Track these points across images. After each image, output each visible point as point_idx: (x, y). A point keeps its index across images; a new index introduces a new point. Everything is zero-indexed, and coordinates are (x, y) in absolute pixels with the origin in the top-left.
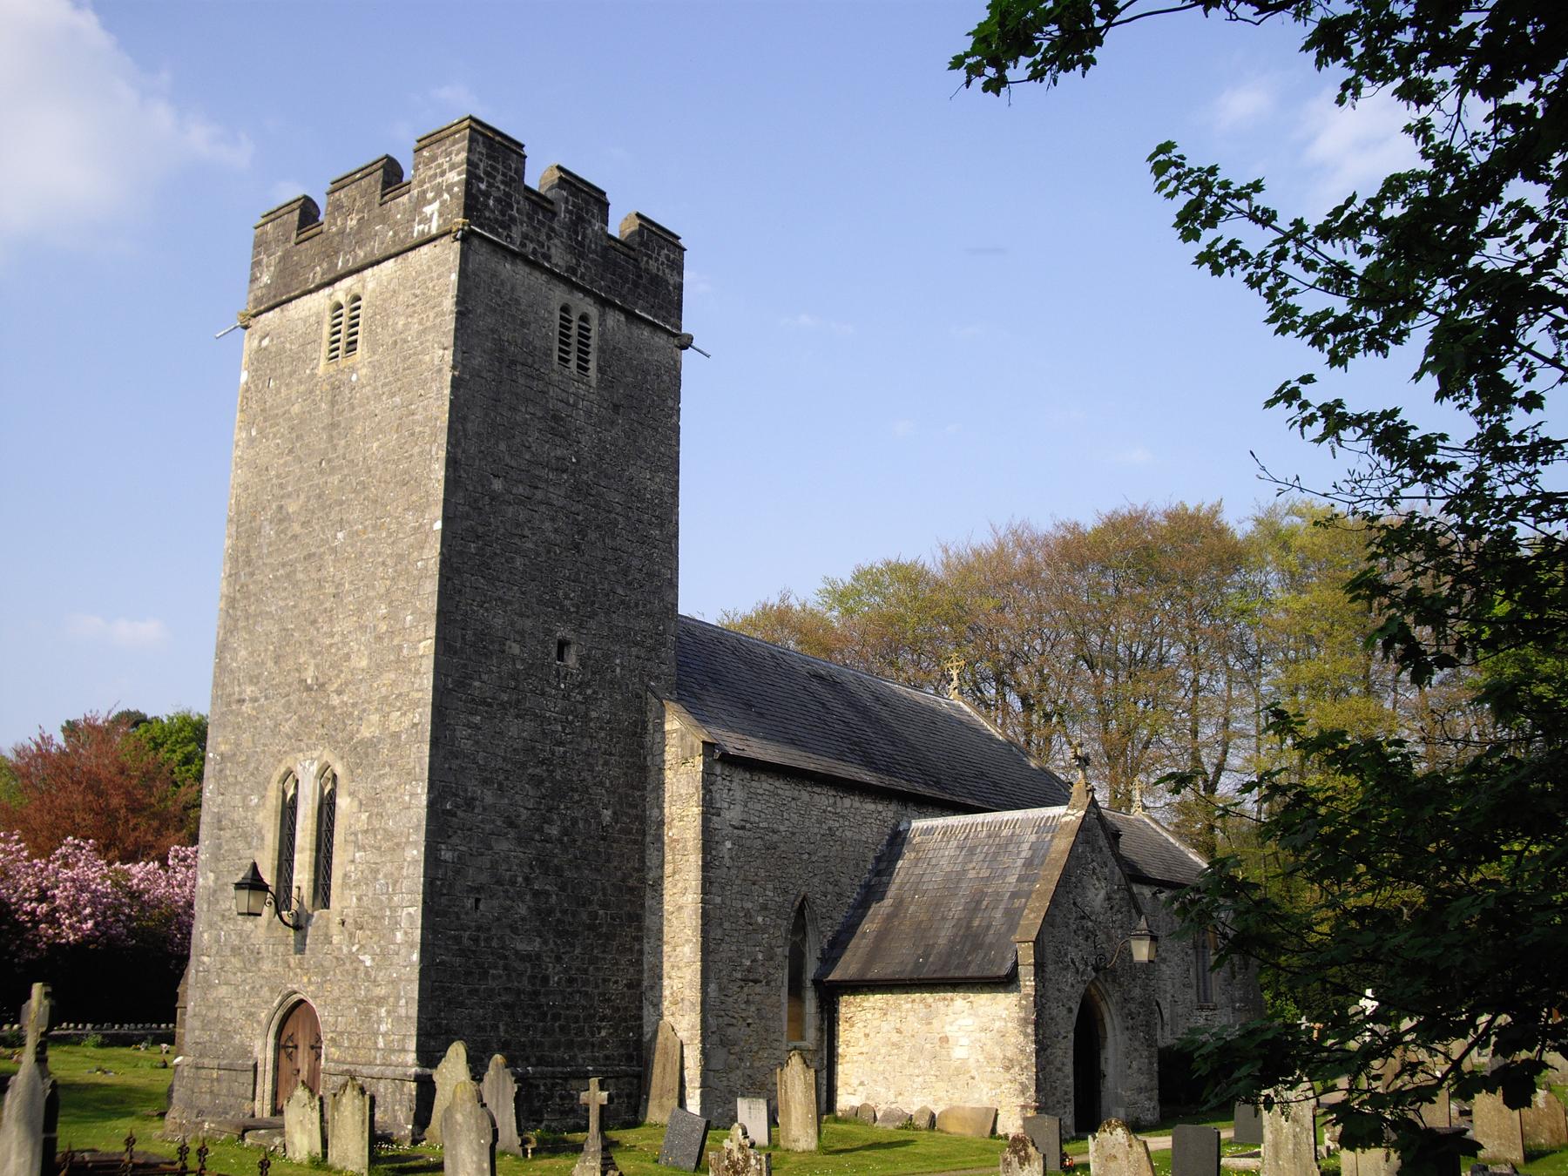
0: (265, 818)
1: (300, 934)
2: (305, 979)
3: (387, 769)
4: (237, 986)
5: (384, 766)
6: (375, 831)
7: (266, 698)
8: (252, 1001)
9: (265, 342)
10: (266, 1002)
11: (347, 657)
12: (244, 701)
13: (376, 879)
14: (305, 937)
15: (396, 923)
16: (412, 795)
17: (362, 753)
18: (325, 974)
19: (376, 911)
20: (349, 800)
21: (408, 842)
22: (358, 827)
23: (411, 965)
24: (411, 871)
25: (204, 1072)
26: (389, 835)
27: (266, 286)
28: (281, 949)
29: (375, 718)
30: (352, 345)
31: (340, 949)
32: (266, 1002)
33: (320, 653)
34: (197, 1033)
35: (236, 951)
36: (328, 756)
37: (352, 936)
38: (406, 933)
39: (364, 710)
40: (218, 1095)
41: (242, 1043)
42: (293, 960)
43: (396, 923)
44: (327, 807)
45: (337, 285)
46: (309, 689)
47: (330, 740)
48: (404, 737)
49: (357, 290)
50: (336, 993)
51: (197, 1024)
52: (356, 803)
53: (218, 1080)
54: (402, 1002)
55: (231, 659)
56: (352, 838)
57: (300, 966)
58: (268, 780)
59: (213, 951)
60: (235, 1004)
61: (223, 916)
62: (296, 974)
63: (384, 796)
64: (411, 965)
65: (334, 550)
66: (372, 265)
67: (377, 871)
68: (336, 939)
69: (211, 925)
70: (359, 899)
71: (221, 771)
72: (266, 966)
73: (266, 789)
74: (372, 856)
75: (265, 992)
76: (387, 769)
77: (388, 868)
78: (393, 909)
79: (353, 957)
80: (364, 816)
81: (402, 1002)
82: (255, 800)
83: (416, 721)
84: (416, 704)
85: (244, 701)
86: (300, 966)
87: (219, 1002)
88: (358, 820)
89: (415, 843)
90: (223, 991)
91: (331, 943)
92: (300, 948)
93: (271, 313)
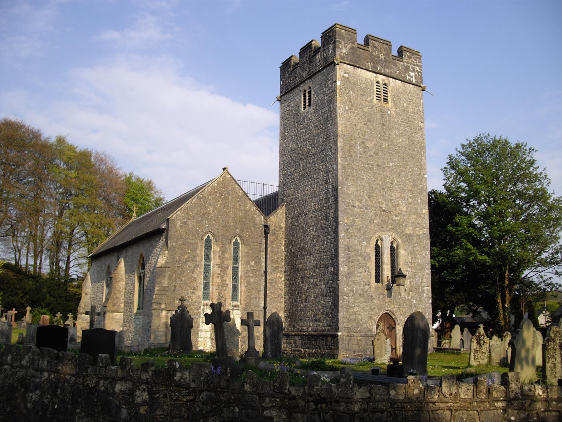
0: (370, 251)
1: (389, 292)
2: (393, 306)
3: (416, 245)
4: (363, 308)
5: (415, 243)
6: (414, 263)
7: (366, 209)
8: (370, 313)
9: (346, 75)
10: (377, 313)
11: (398, 205)
12: (355, 207)
13: (415, 277)
14: (391, 293)
15: (423, 291)
16: (425, 254)
17: (408, 238)
18: (400, 305)
19: (416, 287)
20: (404, 251)
21: (425, 268)
22: (408, 260)
23: (429, 303)
24: (427, 276)
25: (354, 338)
26: (419, 265)
27: (345, 53)
28: (382, 296)
29: (411, 228)
30: (386, 100)
31: (405, 297)
32: (377, 313)
33: (387, 200)
34: (345, 324)
35: (361, 295)
36: (394, 235)
37: (409, 293)
38: (427, 294)
39: (407, 224)
40: (361, 345)
41: (367, 327)
42: (387, 300)
43: (424, 291)
44: (394, 252)
45: (378, 75)
46: (384, 211)
47: (394, 230)
48: (421, 236)
49: (387, 82)
50: (405, 311)
51: (345, 320)
52: (407, 253)
53: (360, 340)
54: (427, 314)
55: (347, 189)
56: (406, 263)
57: (390, 302)
58: (371, 238)
59: (350, 295)
60: (363, 314)
61: (354, 283)
62: (389, 304)
63: (416, 253)
64: (429, 303)
65: (389, 167)
66: (393, 78)
67: (416, 275)
68: (403, 294)
69: (348, 285)
70: (411, 282)
71: (348, 230)
72: (376, 301)
73: (370, 241)
74: (415, 271)
75: (376, 310)
76: (416, 245)
77: (420, 275)
78: (422, 287)
79: (410, 300)
80: (410, 258)
81: (427, 314)
82: (365, 244)
83: (425, 232)
84: (424, 228)
85: (355, 207)
86: (390, 302)
87: (355, 313)
88: (408, 258)
89: (428, 269)
90: (356, 309)
91: (401, 295)
92: (390, 296)
93: (349, 66)
